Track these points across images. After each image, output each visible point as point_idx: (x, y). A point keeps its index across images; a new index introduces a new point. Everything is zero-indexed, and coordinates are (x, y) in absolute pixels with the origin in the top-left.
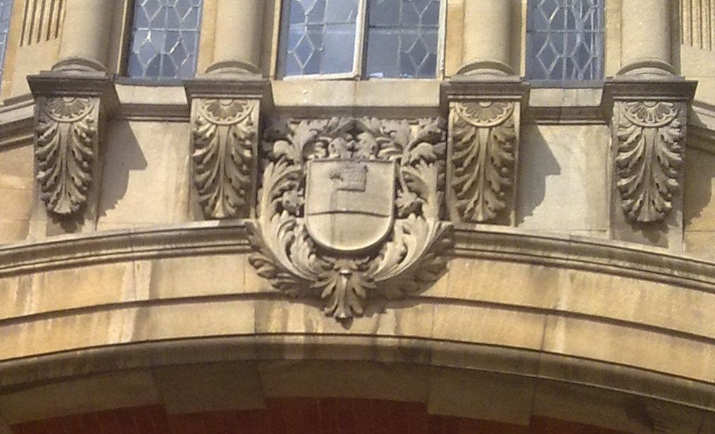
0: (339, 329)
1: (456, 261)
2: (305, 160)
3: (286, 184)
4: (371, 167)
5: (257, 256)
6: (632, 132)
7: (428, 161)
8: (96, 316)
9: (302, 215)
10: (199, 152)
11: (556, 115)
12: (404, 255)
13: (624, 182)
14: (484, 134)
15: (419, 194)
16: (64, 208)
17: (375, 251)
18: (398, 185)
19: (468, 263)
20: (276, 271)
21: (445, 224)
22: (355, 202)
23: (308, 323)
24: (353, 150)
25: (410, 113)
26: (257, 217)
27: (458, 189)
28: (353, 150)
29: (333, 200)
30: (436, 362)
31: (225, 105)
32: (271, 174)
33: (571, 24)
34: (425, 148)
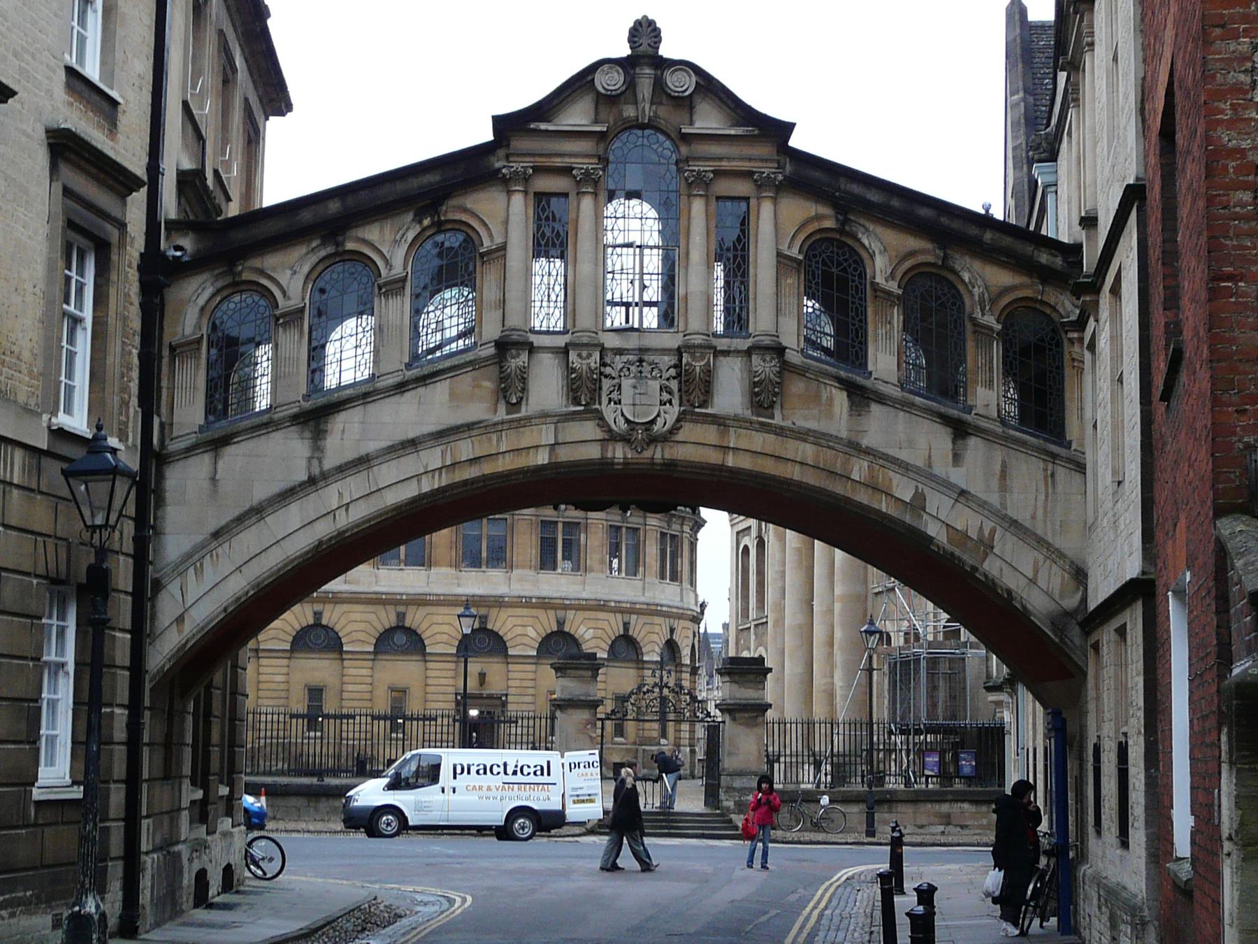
0: (638, 456)
1: (687, 424)
2: (620, 376)
3: (612, 389)
4: (650, 382)
5: (601, 423)
6: (760, 369)
7: (674, 378)
8: (531, 450)
9: (620, 403)
10: (573, 376)
11: (726, 353)
12: (665, 423)
13: (756, 390)
14: (698, 369)
15: (670, 393)
16: (514, 401)
17: (653, 422)
18: (661, 389)
19: (692, 425)
20: (610, 430)
21: (682, 408)
22: (644, 400)
23: (624, 453)
24: (641, 372)
25: (664, 351)
26: (600, 404)
27: (686, 392)
28: (641, 372)
29: (634, 399)
30: (679, 469)
31: (584, 354)
32: (606, 384)
33: (734, 302)
34: (673, 372)
